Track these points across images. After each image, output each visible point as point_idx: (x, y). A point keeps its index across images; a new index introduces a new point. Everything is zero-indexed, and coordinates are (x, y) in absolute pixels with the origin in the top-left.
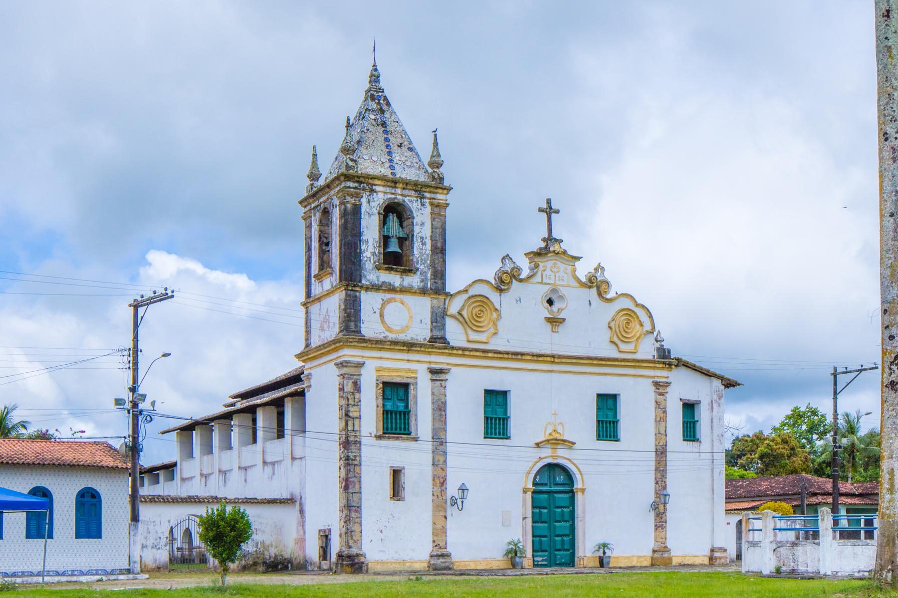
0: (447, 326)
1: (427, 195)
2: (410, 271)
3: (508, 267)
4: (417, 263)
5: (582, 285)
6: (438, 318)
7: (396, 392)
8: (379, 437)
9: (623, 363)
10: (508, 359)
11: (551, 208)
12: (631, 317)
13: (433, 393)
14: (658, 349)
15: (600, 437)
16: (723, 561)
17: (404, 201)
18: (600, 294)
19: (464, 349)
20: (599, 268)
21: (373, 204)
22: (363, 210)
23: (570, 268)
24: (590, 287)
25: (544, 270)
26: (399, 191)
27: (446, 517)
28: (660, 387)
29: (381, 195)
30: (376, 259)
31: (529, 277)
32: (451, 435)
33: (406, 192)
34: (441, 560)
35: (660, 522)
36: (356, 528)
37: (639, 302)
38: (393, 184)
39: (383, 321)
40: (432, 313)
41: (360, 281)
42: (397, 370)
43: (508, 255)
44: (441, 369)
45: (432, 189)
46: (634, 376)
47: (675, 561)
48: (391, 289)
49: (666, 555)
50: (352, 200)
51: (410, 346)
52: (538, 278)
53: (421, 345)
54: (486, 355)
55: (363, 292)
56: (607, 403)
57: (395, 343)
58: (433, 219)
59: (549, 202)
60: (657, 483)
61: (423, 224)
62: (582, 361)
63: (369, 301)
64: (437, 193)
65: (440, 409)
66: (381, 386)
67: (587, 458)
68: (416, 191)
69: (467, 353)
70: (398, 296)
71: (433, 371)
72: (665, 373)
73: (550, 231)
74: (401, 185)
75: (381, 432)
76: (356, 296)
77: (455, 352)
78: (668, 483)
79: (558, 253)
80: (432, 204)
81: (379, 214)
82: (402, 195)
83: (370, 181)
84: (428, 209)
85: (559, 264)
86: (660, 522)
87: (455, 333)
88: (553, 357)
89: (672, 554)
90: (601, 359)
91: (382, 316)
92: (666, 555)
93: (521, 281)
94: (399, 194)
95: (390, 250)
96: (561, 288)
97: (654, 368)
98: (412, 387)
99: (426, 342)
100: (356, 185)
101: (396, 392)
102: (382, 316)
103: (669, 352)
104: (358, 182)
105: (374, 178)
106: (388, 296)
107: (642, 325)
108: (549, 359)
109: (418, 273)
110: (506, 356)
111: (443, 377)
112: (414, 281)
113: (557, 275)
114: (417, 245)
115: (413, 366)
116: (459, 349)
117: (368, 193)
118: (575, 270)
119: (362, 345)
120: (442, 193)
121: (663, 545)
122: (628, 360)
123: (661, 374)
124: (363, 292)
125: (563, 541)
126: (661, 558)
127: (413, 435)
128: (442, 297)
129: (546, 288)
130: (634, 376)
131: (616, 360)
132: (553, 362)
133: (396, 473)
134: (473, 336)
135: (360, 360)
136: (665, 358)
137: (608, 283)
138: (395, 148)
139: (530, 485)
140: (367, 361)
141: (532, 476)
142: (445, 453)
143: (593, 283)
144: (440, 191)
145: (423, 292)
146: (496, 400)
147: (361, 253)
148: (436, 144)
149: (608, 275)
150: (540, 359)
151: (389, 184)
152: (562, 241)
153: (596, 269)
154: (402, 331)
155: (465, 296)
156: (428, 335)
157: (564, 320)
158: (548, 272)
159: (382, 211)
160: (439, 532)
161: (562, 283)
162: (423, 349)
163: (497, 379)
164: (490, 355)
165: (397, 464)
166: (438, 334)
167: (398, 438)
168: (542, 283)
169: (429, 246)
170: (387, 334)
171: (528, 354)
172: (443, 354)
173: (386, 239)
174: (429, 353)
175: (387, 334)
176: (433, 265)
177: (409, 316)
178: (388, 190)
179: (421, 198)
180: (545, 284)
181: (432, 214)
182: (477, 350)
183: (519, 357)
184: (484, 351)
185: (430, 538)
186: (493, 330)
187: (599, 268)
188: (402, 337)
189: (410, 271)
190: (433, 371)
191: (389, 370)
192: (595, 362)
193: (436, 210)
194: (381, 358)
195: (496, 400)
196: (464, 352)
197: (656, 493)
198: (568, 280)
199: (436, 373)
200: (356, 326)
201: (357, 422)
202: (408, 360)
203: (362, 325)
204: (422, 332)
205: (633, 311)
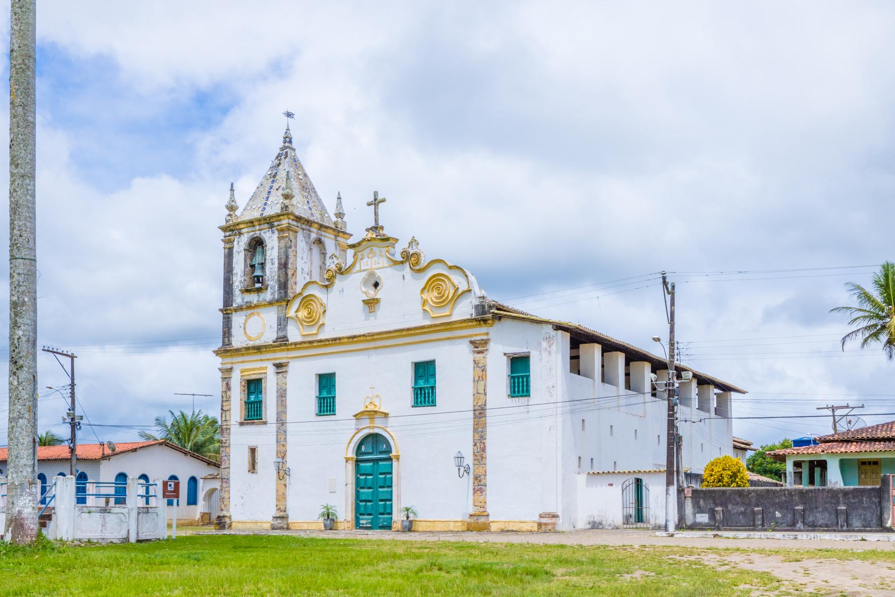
1: (276, 224)
5: (395, 263)
6: (283, 322)
7: (254, 385)
8: (242, 424)
9: (432, 329)
15: (417, 404)
16: (550, 527)
20: (413, 242)
21: (241, 244)
24: (402, 262)
27: (285, 485)
28: (479, 346)
32: (290, 417)
34: (279, 521)
35: (479, 487)
36: (226, 495)
39: (245, 333)
42: (254, 369)
46: (448, 339)
47: (494, 527)
48: (250, 307)
49: (482, 520)
51: (258, 349)
52: (357, 267)
53: (266, 347)
56: (424, 370)
57: (247, 349)
60: (475, 445)
61: (273, 248)
62: (392, 335)
63: (237, 319)
65: (282, 395)
67: (404, 427)
69: (298, 346)
70: (255, 311)
71: (278, 366)
75: (242, 420)
78: (487, 445)
85: (375, 249)
86: (479, 487)
87: (294, 334)
89: (491, 519)
90: (408, 329)
92: (482, 520)
93: (342, 274)
101: (254, 385)
105: (238, 224)
106: (250, 312)
108: (362, 338)
113: (373, 259)
115: (263, 364)
116: (291, 344)
121: (482, 510)
122: (436, 326)
125: (365, 506)
126: (478, 523)
127: (264, 420)
129: (363, 275)
130: (448, 339)
131: (431, 326)
133: (253, 451)
135: (229, 366)
138: (273, 191)
139: (351, 454)
140: (235, 366)
141: (352, 445)
142: (285, 432)
144: (282, 217)
145: (270, 303)
146: (326, 381)
154: (259, 338)
160: (281, 497)
161: (377, 266)
164: (315, 344)
165: (253, 444)
166: (281, 334)
167: (253, 423)
168: (360, 271)
169: (276, 265)
171: (344, 338)
172: (283, 350)
173: (253, 266)
174: (274, 351)
176: (279, 281)
180: (364, 271)
184: (310, 342)
185: (274, 502)
186: (321, 322)
187: (413, 242)
188: (258, 343)
190: (278, 366)
194: (243, 362)
195: (326, 381)
196: (297, 345)
197: (475, 455)
198: (384, 262)
200: (229, 340)
201: (228, 413)
204: (270, 336)
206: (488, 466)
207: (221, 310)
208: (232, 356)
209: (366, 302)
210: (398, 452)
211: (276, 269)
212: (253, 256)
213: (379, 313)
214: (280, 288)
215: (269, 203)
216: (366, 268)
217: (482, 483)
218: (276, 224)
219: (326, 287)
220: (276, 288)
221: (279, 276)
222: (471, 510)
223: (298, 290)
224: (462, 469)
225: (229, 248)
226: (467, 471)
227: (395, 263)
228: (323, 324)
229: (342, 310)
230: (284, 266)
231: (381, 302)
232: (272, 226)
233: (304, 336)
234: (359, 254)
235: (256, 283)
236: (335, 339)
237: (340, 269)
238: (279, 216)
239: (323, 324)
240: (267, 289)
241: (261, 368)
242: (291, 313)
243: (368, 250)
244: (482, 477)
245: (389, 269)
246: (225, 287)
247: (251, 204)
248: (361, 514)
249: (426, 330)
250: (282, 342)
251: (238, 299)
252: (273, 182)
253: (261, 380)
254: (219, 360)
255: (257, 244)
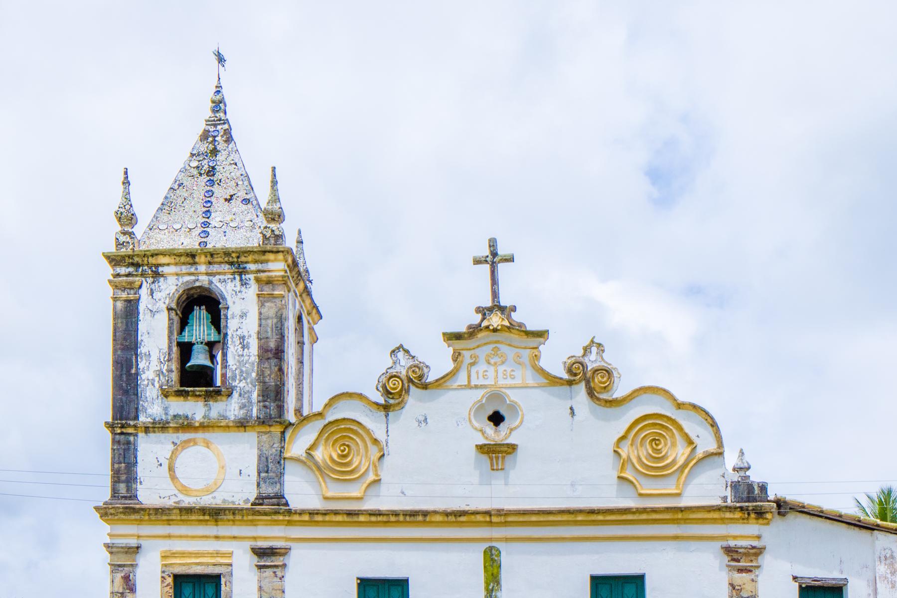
0: (287, 478)
1: (252, 267)
2: (215, 394)
3: (403, 365)
4: (234, 379)
6: (271, 467)
9: (644, 516)
10: (398, 522)
11: (494, 254)
12: (659, 427)
13: (260, 588)
14: (735, 486)
17: (211, 282)
18: (591, 393)
19: (312, 513)
21: (157, 295)
22: (142, 307)
23: (526, 354)
24: (570, 383)
25: (473, 364)
26: (202, 268)
29: (172, 280)
30: (163, 380)
31: (441, 382)
33: (215, 268)
37: (681, 397)
38: (189, 259)
39: (173, 477)
40: (260, 457)
41: (136, 418)
42: (197, 554)
43: (401, 346)
44: (272, 548)
45: (256, 257)
46: (676, 538)
48: (186, 425)
50: (124, 295)
51: (215, 514)
52: (462, 378)
53: (234, 511)
54: (355, 519)
55: (141, 435)
58: (262, 305)
59: (493, 244)
61: (243, 315)
62: (551, 518)
64: (267, 261)
66: (170, 580)
68: (231, 264)
69: (319, 518)
70: (199, 435)
71: (261, 553)
72: (752, 528)
73: (495, 295)
74: (203, 259)
76: (129, 443)
77: (296, 518)
79: (495, 330)
80: (258, 280)
81: (170, 309)
82: (207, 274)
83: (152, 260)
84: (253, 289)
85: (504, 348)
87: (301, 491)
88: (488, 513)
90: (592, 512)
91: (171, 469)
93: (425, 387)
94: (201, 276)
95: (194, 362)
96: (508, 392)
97: (723, 521)
98: (223, 580)
99: (249, 506)
100: (131, 269)
102: (171, 469)
103: (763, 488)
104: (132, 264)
105: (155, 254)
107: (690, 442)
108: (479, 518)
109: (236, 395)
110: (393, 519)
111: (278, 561)
112: (232, 408)
113: (501, 369)
114: (233, 349)
116: (301, 513)
117: (150, 280)
118: (537, 357)
119: (133, 517)
120: (276, 260)
122: (654, 510)
123: (743, 532)
124: (141, 435)
128: (277, 430)
129: (479, 394)
130: (676, 538)
132: (491, 523)
134: (334, 490)
136: (752, 501)
137: (608, 372)
140: (143, 542)
143: (575, 375)
144: (271, 256)
145: (242, 425)
147: (137, 374)
148: (274, 183)
149: (610, 359)
150: (463, 519)
151: (183, 259)
152: (514, 309)
153: (587, 350)
154: (209, 491)
155: (319, 424)
156: (252, 493)
157: (513, 448)
158: (482, 367)
159: (174, 305)
161: (509, 382)
162: (238, 517)
163: (382, 562)
164: (362, 518)
166: (269, 490)
168: (469, 386)
169: (254, 349)
170: (181, 497)
172: (276, 523)
174: (253, 523)
175: (181, 497)
176: (261, 379)
177: (222, 467)
178: (185, 269)
179: (240, 274)
180: (476, 387)
181: (259, 296)
182: (336, 513)
183: (420, 518)
184: (350, 513)
186: (371, 477)
188: (207, 501)
189: (218, 393)
190: (261, 553)
191: (183, 554)
192: (580, 518)
193: (267, 290)
194: (169, 537)
196: (313, 516)
199: (267, 555)
202: (217, 537)
203: (139, 486)
204: (241, 490)
205: (669, 419)
207: (111, 426)
208: (140, 522)
209: (481, 448)
211: (254, 359)
212: (184, 323)
213: (513, 474)
214: (265, 395)
215: (213, 223)
216: (481, 382)
218: (252, 267)
219: (386, 408)
220: (255, 396)
221: (261, 373)
223: (318, 407)
225: (129, 301)
227: (554, 381)
228: (377, 482)
229: (427, 457)
230: (273, 354)
231: (519, 451)
232: (241, 271)
233: (326, 498)
234: (466, 354)
235: (196, 379)
236: (414, 514)
237: (421, 377)
238: (264, 252)
239: (377, 482)
240: (230, 395)
241: (218, 554)
242: (298, 446)
243: (488, 349)
245: (537, 392)
246: (117, 379)
247: (164, 217)
249: (630, 517)
250: (271, 505)
251: (153, 406)
252: (212, 183)
253: (215, 579)
254: (106, 528)
255: (200, 303)
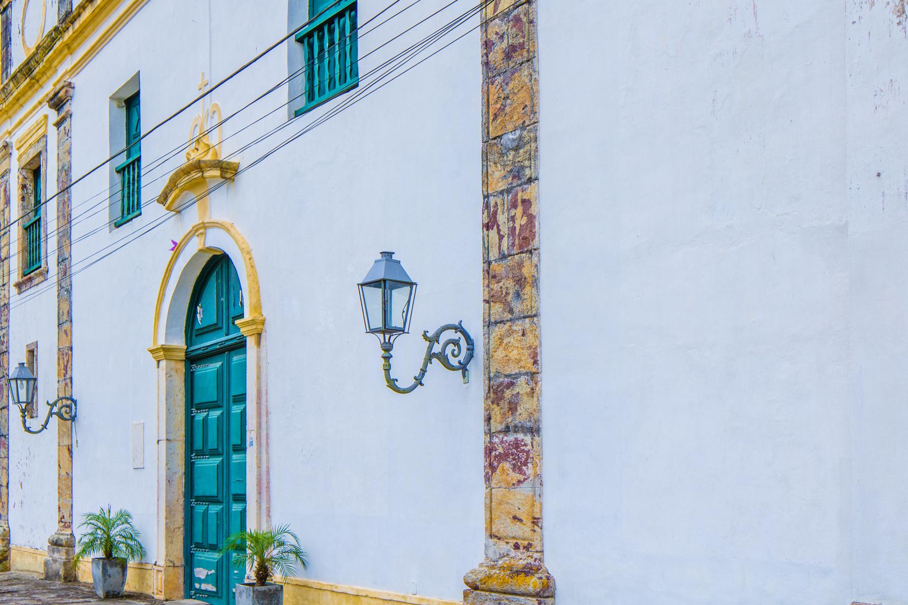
121: (521, 559)
197: (490, 275)
206: (546, 322)
210: (258, 307)
217: (521, 416)
222: (474, 554)
224: (409, 353)
226: (450, 350)
244: (521, 386)
248: (199, 546)
